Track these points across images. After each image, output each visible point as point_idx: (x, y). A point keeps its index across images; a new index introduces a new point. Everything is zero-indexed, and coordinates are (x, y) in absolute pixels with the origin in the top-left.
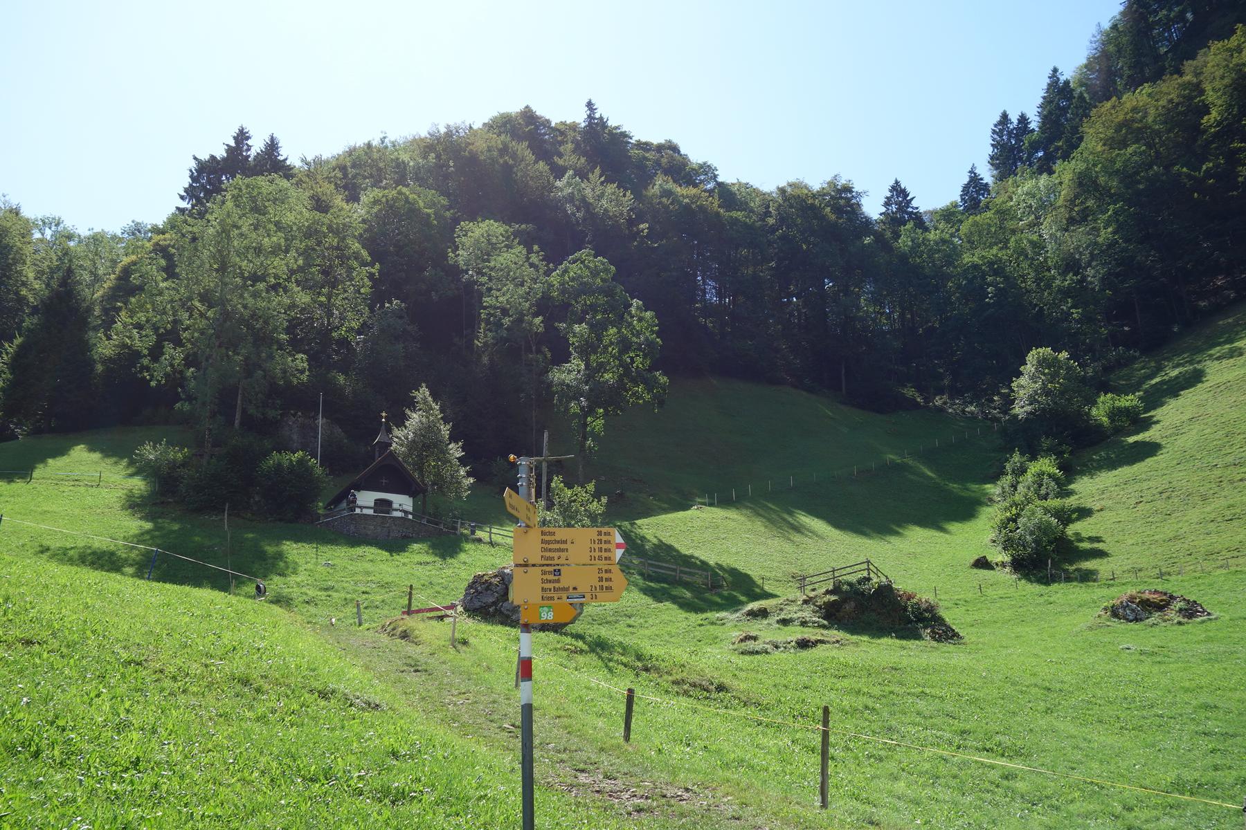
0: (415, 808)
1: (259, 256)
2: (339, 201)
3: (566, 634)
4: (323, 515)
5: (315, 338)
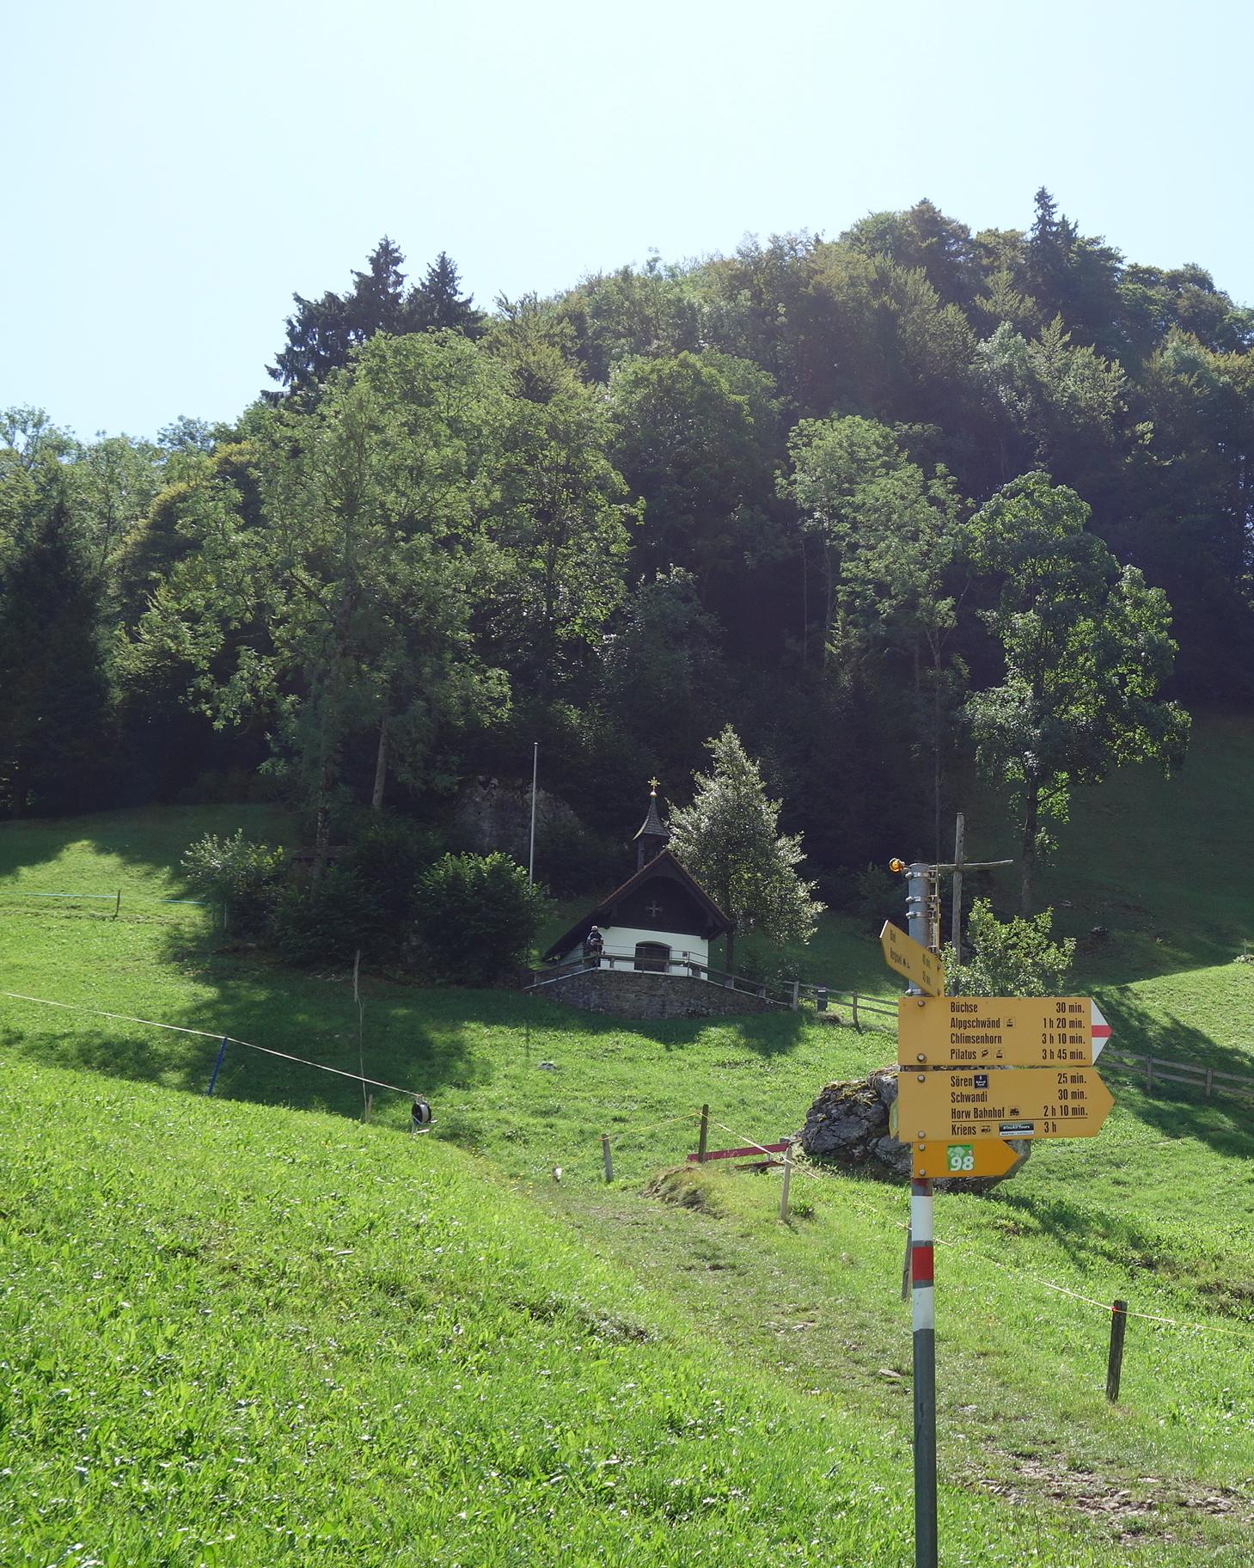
0: (713, 1526)
1: (418, 484)
2: (568, 379)
3: (997, 1198)
4: (540, 973)
5: (523, 639)
